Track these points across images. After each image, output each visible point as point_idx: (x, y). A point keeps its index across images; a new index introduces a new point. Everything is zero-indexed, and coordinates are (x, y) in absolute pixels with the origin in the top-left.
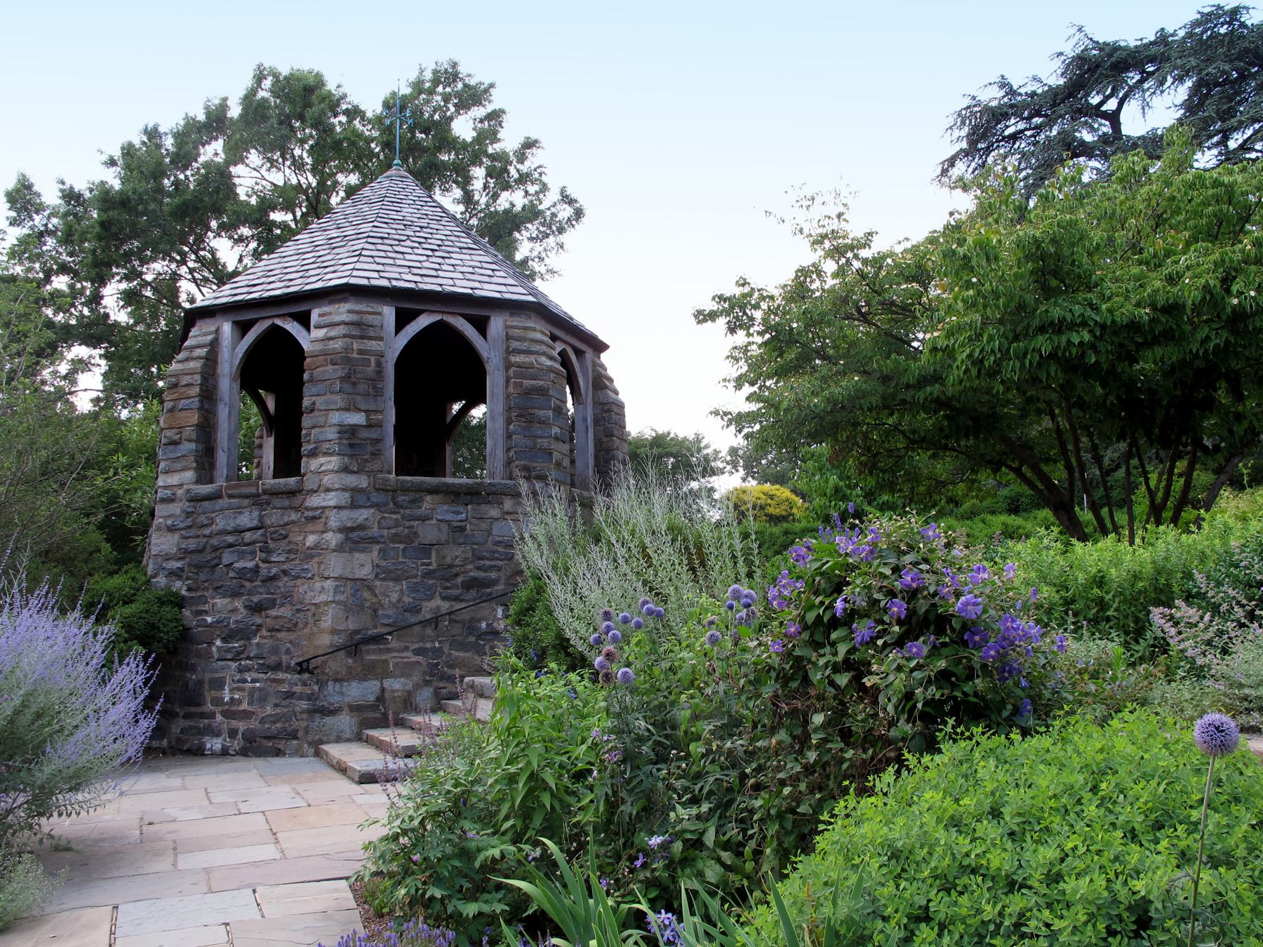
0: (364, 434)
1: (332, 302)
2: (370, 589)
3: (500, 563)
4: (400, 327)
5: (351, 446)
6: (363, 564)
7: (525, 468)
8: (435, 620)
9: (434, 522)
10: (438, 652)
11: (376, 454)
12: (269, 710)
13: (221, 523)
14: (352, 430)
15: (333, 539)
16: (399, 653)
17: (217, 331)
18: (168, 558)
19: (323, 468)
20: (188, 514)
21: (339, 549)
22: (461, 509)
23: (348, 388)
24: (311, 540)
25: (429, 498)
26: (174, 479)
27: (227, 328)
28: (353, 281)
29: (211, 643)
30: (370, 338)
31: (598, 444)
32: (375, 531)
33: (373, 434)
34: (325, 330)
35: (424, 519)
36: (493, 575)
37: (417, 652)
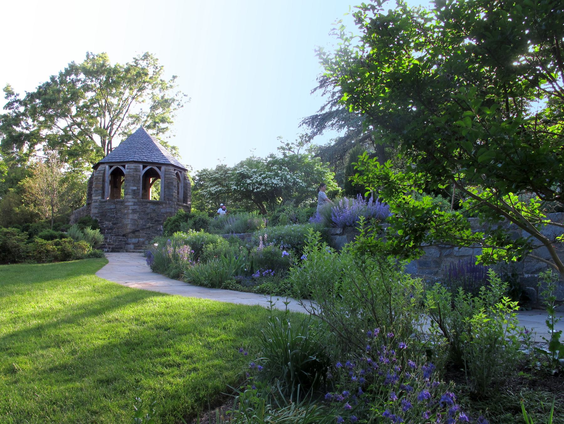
0: (136, 191)
2: (137, 221)
4: (143, 169)
6: (136, 216)
7: (168, 198)
8: (149, 228)
10: (149, 234)
11: (139, 195)
12: (117, 244)
13: (107, 207)
14: (134, 190)
15: (130, 211)
16: (142, 233)
17: (105, 167)
18: (95, 214)
20: (100, 205)
21: (131, 213)
23: (133, 182)
24: (126, 211)
26: (97, 198)
27: (107, 167)
28: (135, 160)
29: (105, 231)
31: (184, 192)
32: (138, 210)
33: (138, 191)
35: (148, 208)
36: (161, 219)
37: (145, 234)
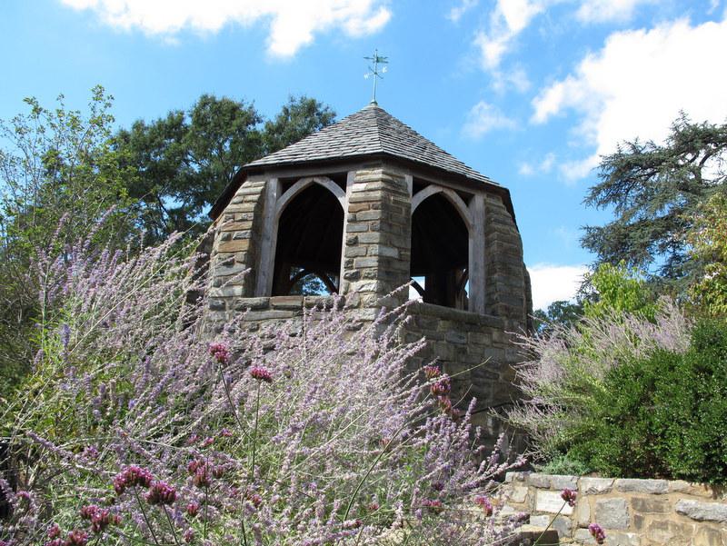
1: (366, 167)
3: (490, 381)
4: (415, 192)
5: (388, 273)
7: (507, 309)
9: (445, 342)
19: (363, 289)
22: (463, 334)
25: (441, 323)
27: (274, 183)
30: (400, 194)
34: (365, 184)
